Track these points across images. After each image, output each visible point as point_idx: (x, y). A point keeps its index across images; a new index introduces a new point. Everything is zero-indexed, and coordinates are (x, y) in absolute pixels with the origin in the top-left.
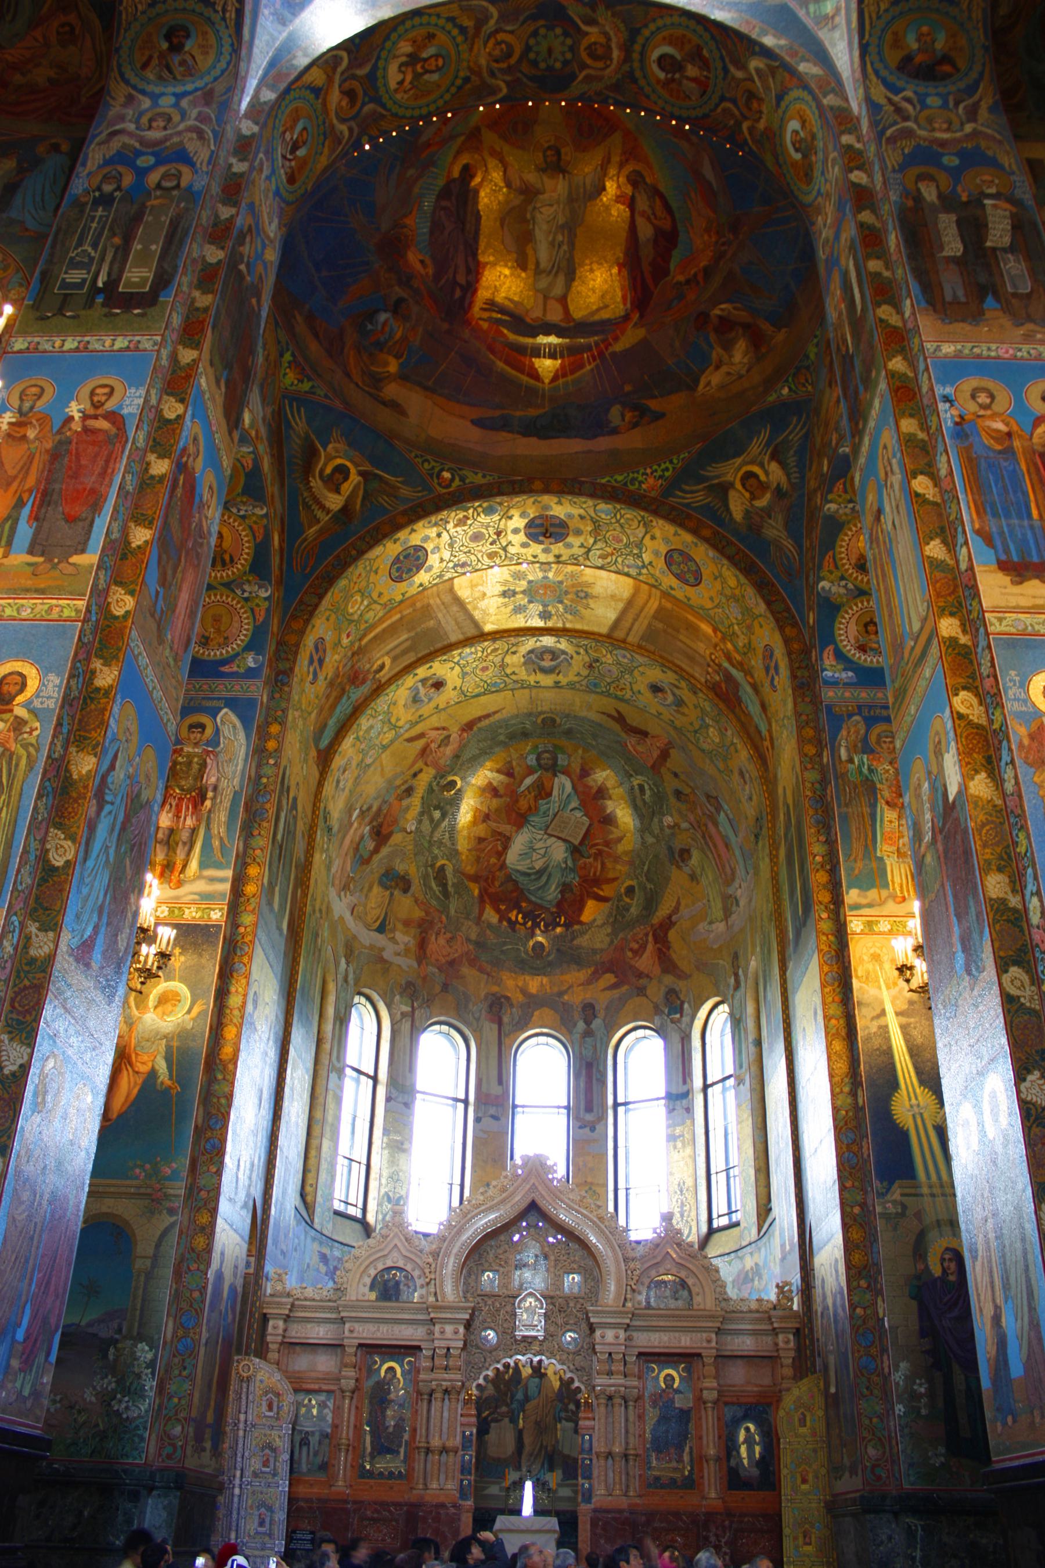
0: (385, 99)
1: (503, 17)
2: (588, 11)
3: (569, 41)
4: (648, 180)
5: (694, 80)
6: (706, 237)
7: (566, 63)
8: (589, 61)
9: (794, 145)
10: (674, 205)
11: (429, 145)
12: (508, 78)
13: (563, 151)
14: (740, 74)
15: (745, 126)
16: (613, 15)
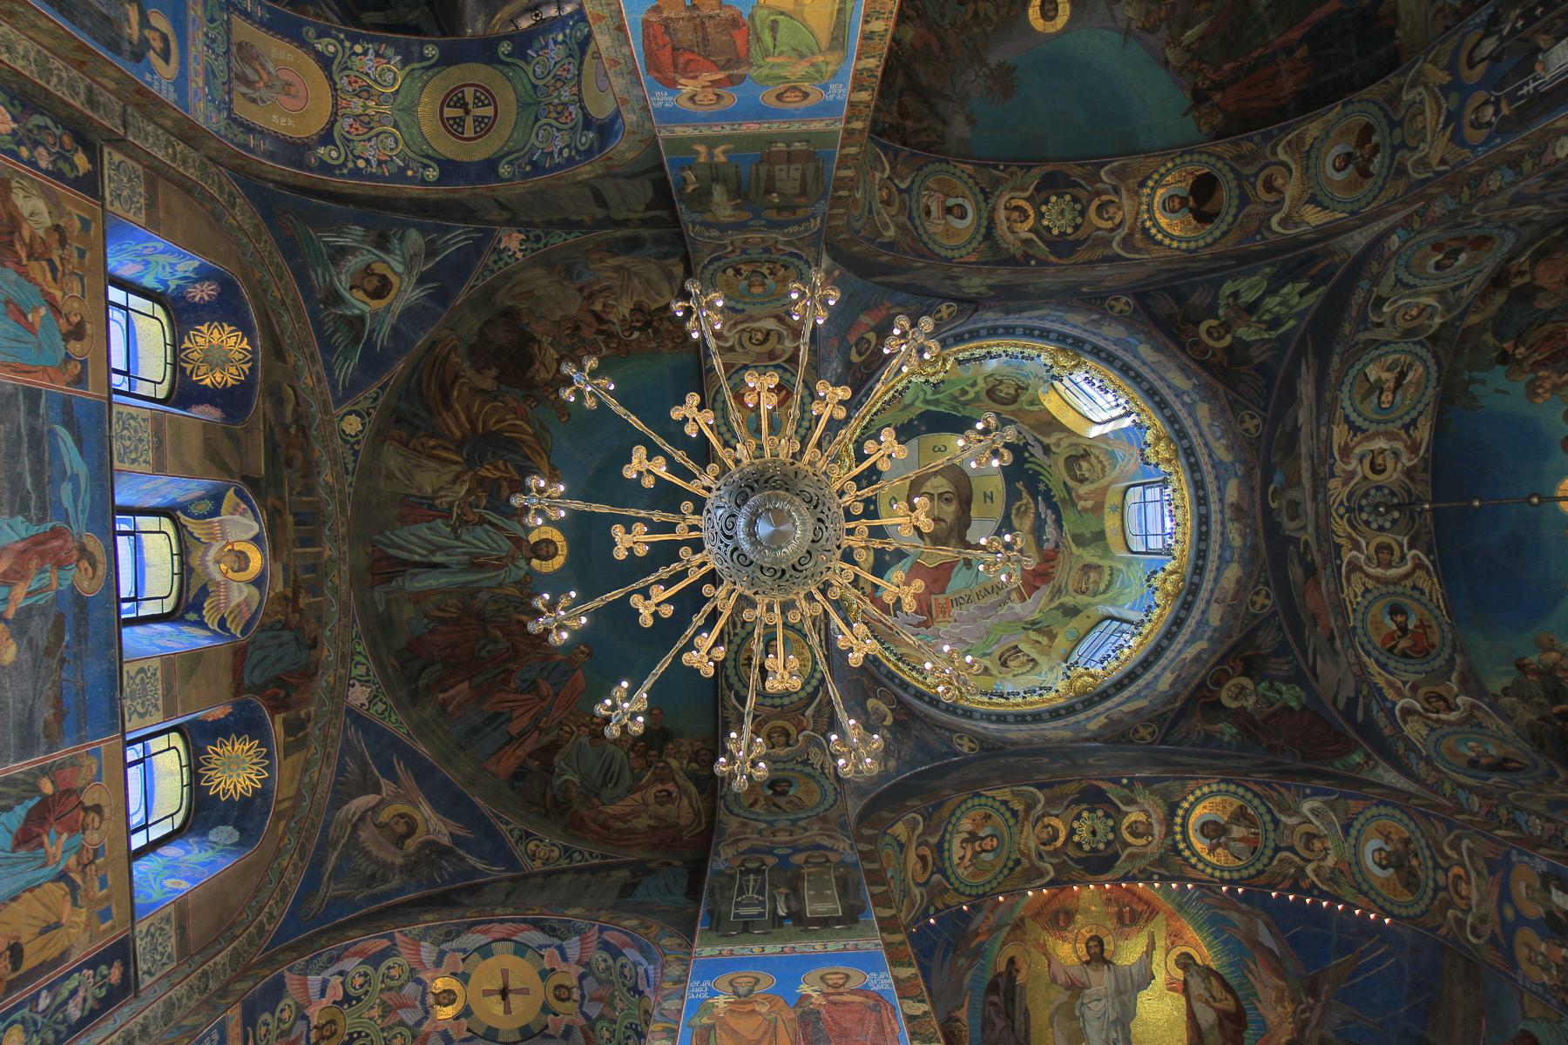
0: (949, 872)
1: (1050, 802)
2: (1127, 792)
3: (1111, 822)
4: (1198, 960)
5: (1240, 840)
6: (1280, 1009)
7: (1108, 844)
8: (1130, 839)
9: (1379, 865)
10: (1233, 982)
11: (977, 934)
12: (1055, 861)
13: (1105, 940)
14: (1292, 821)
15: (1309, 869)
16: (1152, 793)
